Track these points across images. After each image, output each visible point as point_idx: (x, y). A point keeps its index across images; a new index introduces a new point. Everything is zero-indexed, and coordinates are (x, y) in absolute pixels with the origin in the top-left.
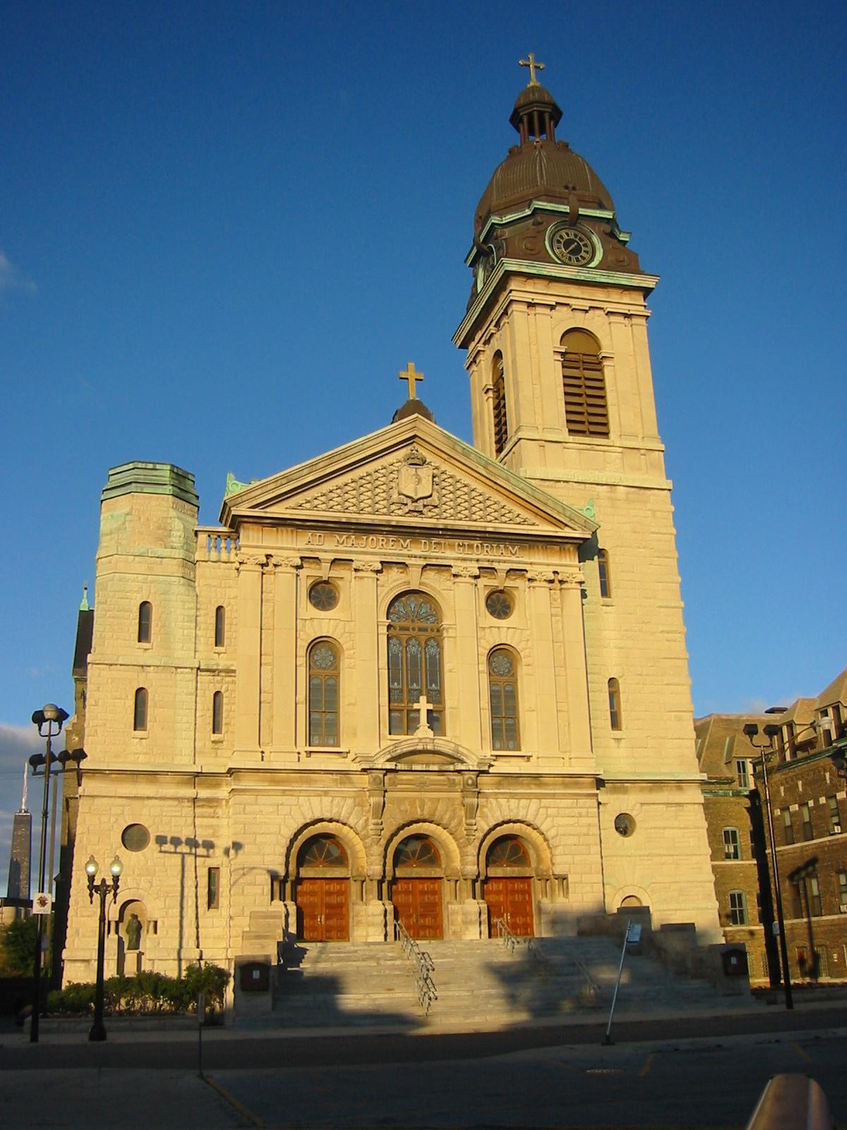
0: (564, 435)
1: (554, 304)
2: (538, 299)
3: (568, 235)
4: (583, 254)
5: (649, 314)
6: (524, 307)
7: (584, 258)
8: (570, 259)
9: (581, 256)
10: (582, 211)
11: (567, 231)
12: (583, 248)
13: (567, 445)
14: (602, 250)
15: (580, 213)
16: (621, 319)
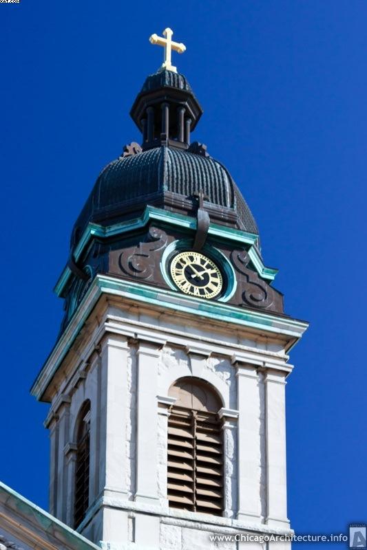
0: (162, 506)
1: (165, 343)
2: (144, 335)
3: (192, 259)
4: (210, 285)
5: (290, 370)
6: (125, 344)
7: (210, 291)
8: (192, 289)
9: (208, 289)
10: (211, 231)
11: (191, 254)
12: (211, 279)
13: (163, 519)
14: (236, 283)
15: (210, 231)
16: (254, 373)
